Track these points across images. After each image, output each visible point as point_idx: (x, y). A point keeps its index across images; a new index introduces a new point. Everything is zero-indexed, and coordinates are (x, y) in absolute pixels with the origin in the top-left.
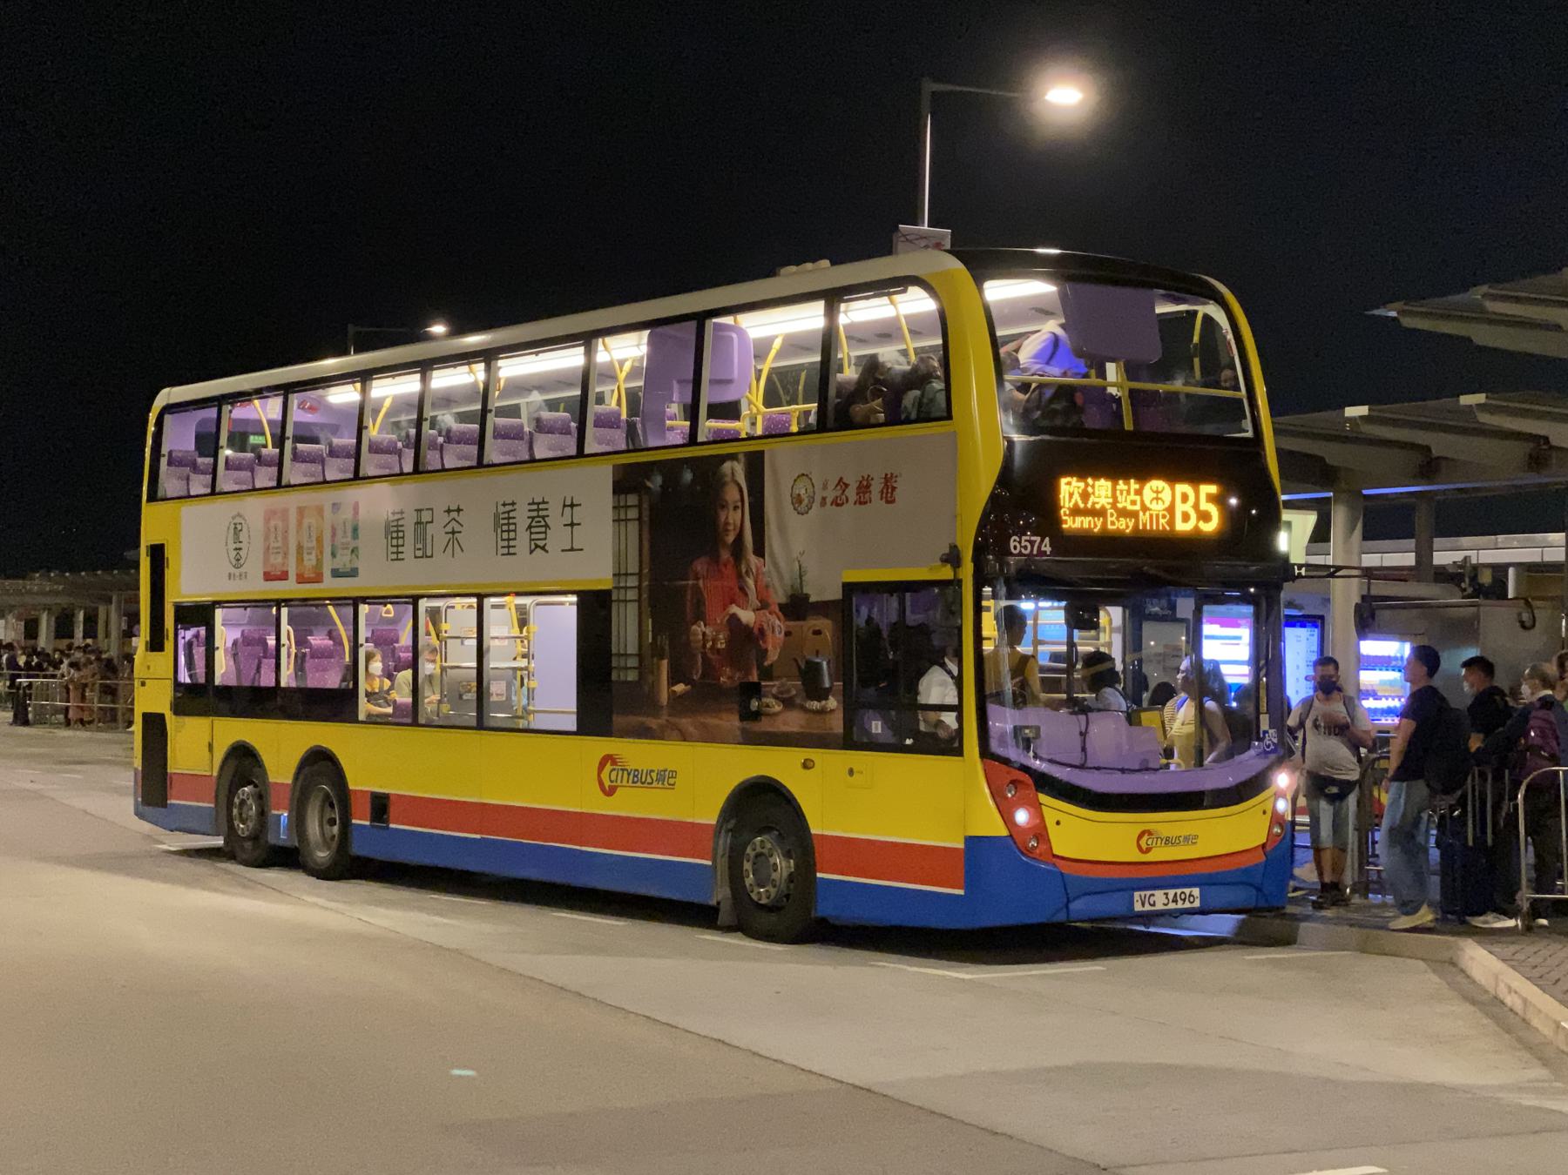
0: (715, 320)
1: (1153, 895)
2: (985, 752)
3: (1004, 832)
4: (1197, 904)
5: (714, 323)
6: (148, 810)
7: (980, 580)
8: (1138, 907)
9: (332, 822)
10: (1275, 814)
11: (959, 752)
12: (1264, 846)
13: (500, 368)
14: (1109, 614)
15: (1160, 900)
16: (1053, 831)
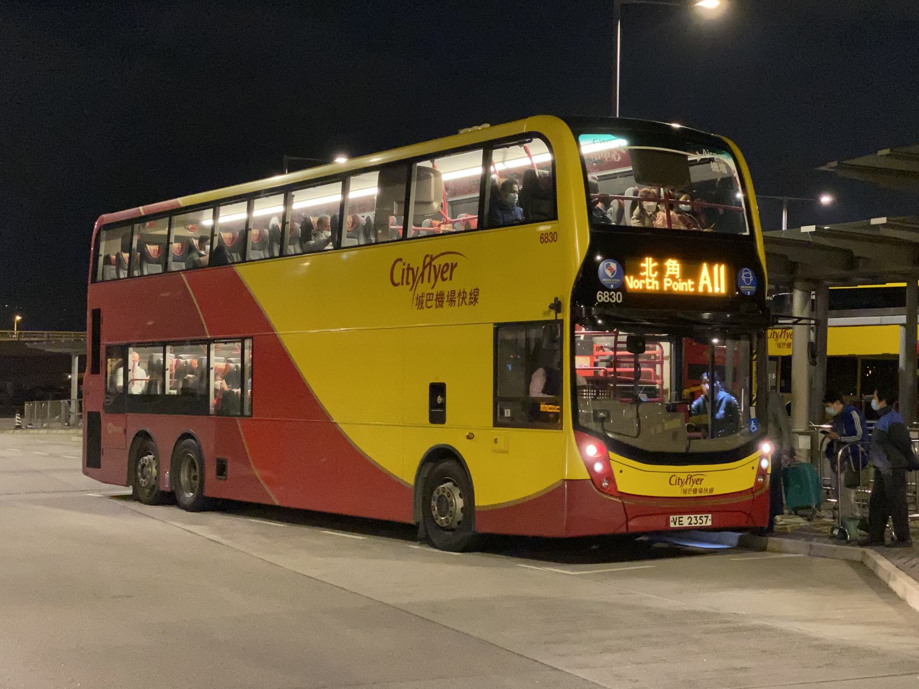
0: (419, 164)
1: (682, 517)
2: (576, 426)
3: (588, 477)
4: (709, 523)
5: (419, 167)
6: (90, 470)
7: (576, 320)
8: (672, 525)
9: (195, 478)
10: (760, 467)
11: (560, 427)
12: (752, 488)
13: (294, 196)
14: (661, 346)
15: (686, 521)
16: (618, 477)
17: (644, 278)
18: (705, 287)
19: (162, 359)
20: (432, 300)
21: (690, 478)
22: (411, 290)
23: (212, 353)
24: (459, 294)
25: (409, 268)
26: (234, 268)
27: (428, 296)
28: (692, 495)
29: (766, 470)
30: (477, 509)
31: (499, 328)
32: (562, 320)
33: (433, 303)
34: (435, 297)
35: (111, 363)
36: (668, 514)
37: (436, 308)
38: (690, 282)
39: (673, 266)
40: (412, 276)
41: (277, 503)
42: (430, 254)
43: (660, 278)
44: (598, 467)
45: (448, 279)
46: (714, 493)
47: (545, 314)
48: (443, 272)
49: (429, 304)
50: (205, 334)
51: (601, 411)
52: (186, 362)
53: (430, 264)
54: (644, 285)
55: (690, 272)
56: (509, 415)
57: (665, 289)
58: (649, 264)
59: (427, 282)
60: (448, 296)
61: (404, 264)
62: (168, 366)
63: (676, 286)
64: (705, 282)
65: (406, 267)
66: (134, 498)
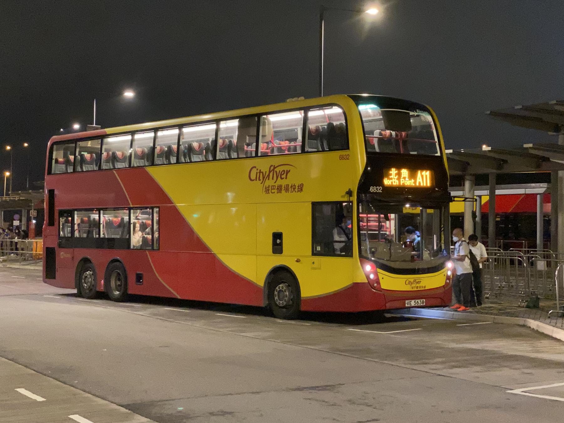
2: (361, 256)
3: (367, 281)
8: (407, 305)
10: (447, 274)
12: (444, 286)
15: (413, 303)
16: (381, 281)
17: (391, 179)
18: (420, 183)
19: (98, 218)
20: (275, 189)
21: (415, 281)
22: (262, 183)
23: (132, 215)
24: (292, 186)
25: (260, 172)
26: (146, 169)
27: (272, 187)
28: (416, 290)
29: (450, 276)
30: (302, 299)
31: (315, 205)
32: (352, 202)
33: (276, 191)
34: (276, 188)
35: (62, 220)
36: (404, 299)
37: (277, 193)
38: (413, 181)
39: (405, 172)
40: (262, 177)
41: (179, 297)
42: (273, 165)
43: (399, 179)
44: (372, 276)
45: (285, 177)
46: (426, 288)
47: (343, 196)
48: (281, 175)
49: (273, 191)
50: (130, 205)
51: (372, 248)
52: (109, 219)
53: (273, 170)
54: (392, 183)
55: (413, 175)
56: (320, 250)
57: (401, 184)
58: (393, 171)
59: (272, 180)
60: (284, 187)
61: (257, 170)
62: (101, 222)
63: (406, 183)
64: (420, 181)
65: (258, 171)
66: (79, 295)
